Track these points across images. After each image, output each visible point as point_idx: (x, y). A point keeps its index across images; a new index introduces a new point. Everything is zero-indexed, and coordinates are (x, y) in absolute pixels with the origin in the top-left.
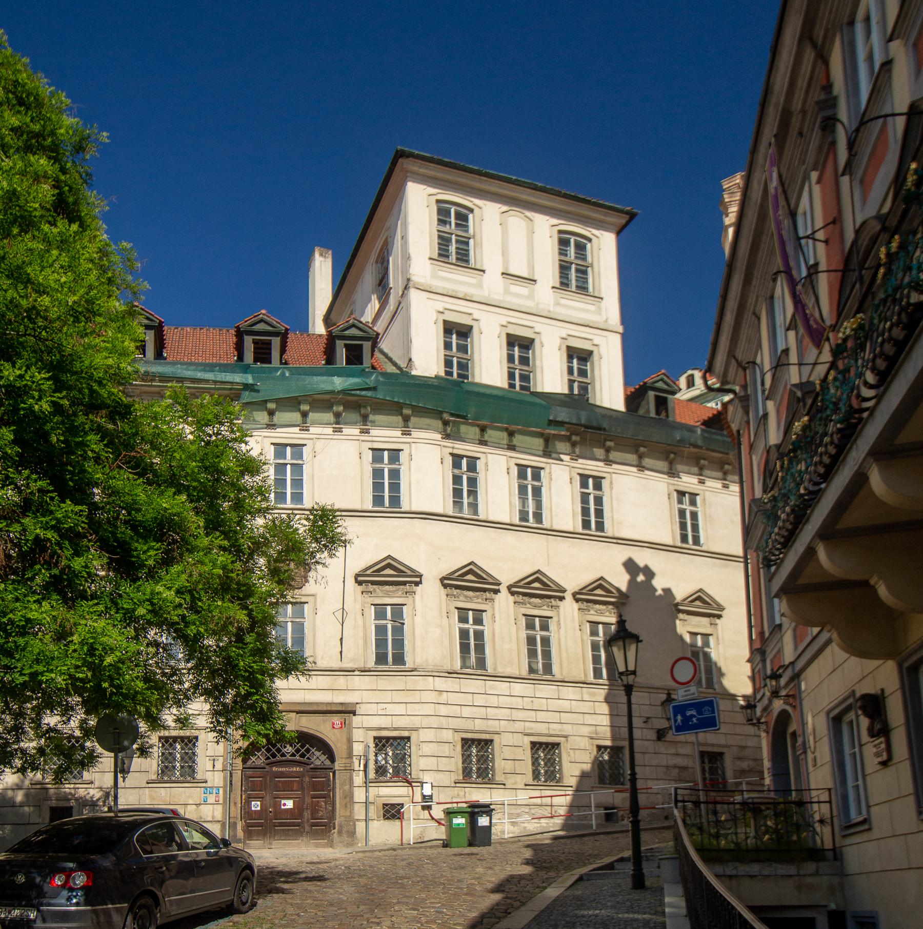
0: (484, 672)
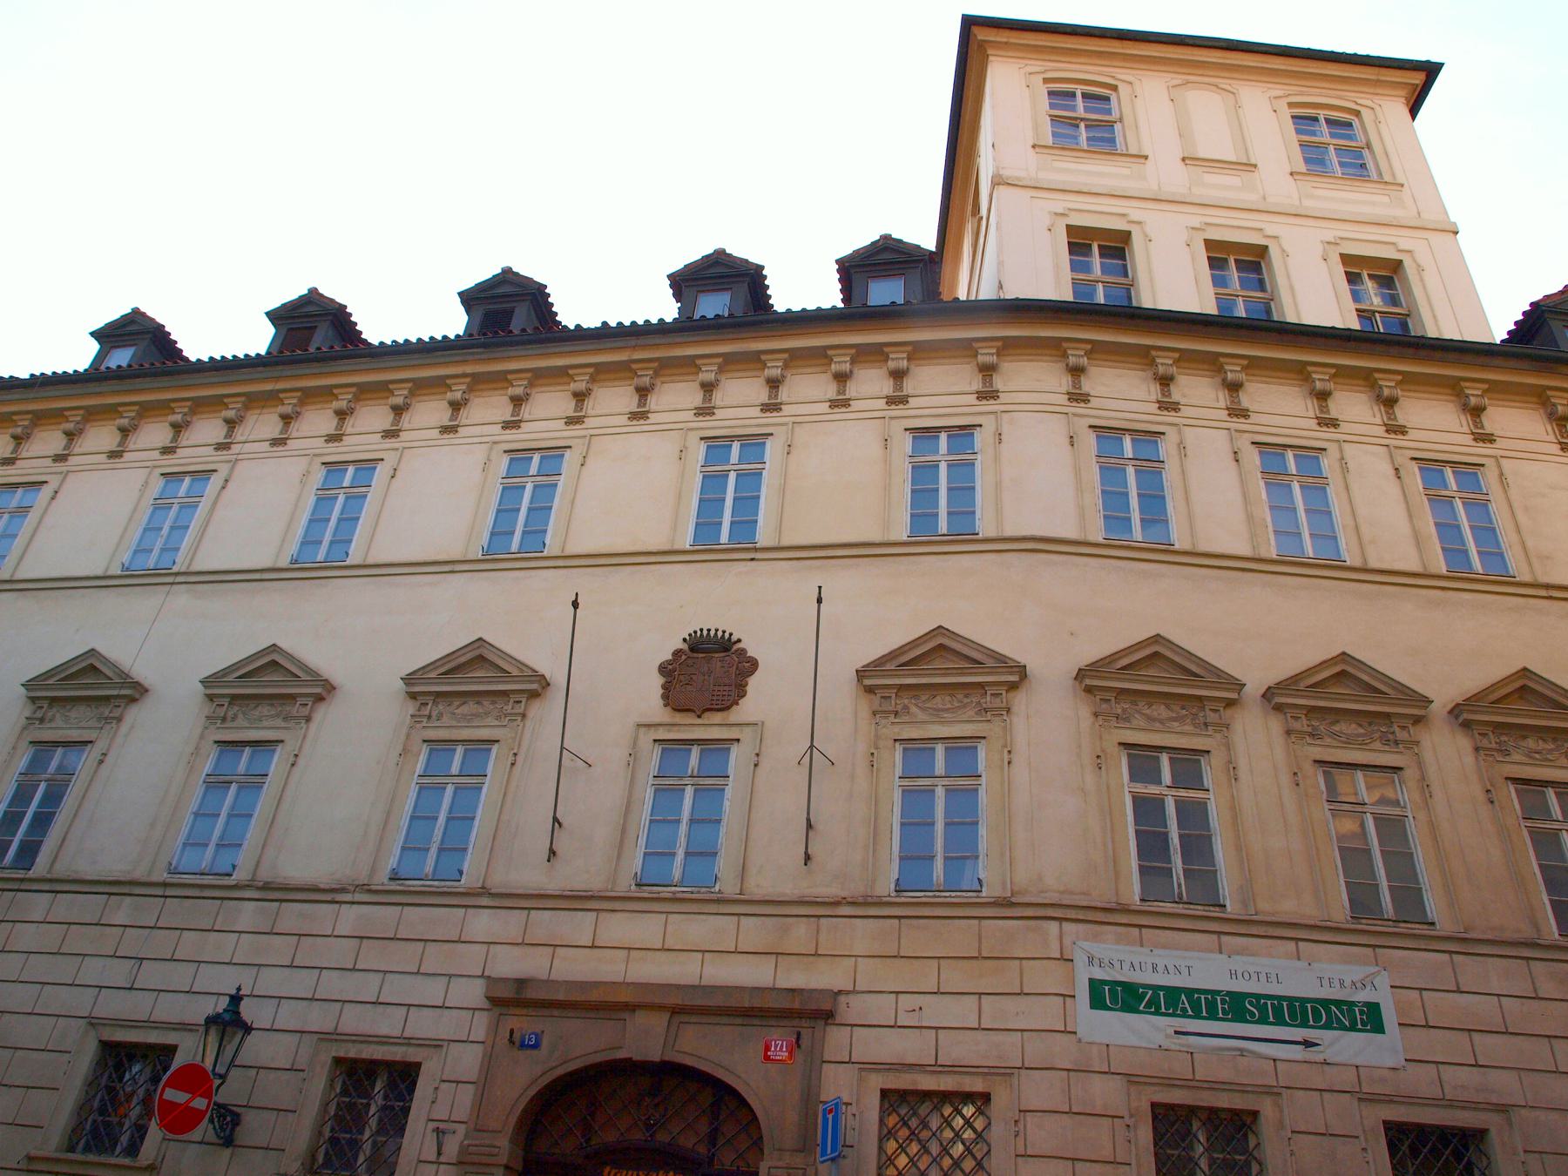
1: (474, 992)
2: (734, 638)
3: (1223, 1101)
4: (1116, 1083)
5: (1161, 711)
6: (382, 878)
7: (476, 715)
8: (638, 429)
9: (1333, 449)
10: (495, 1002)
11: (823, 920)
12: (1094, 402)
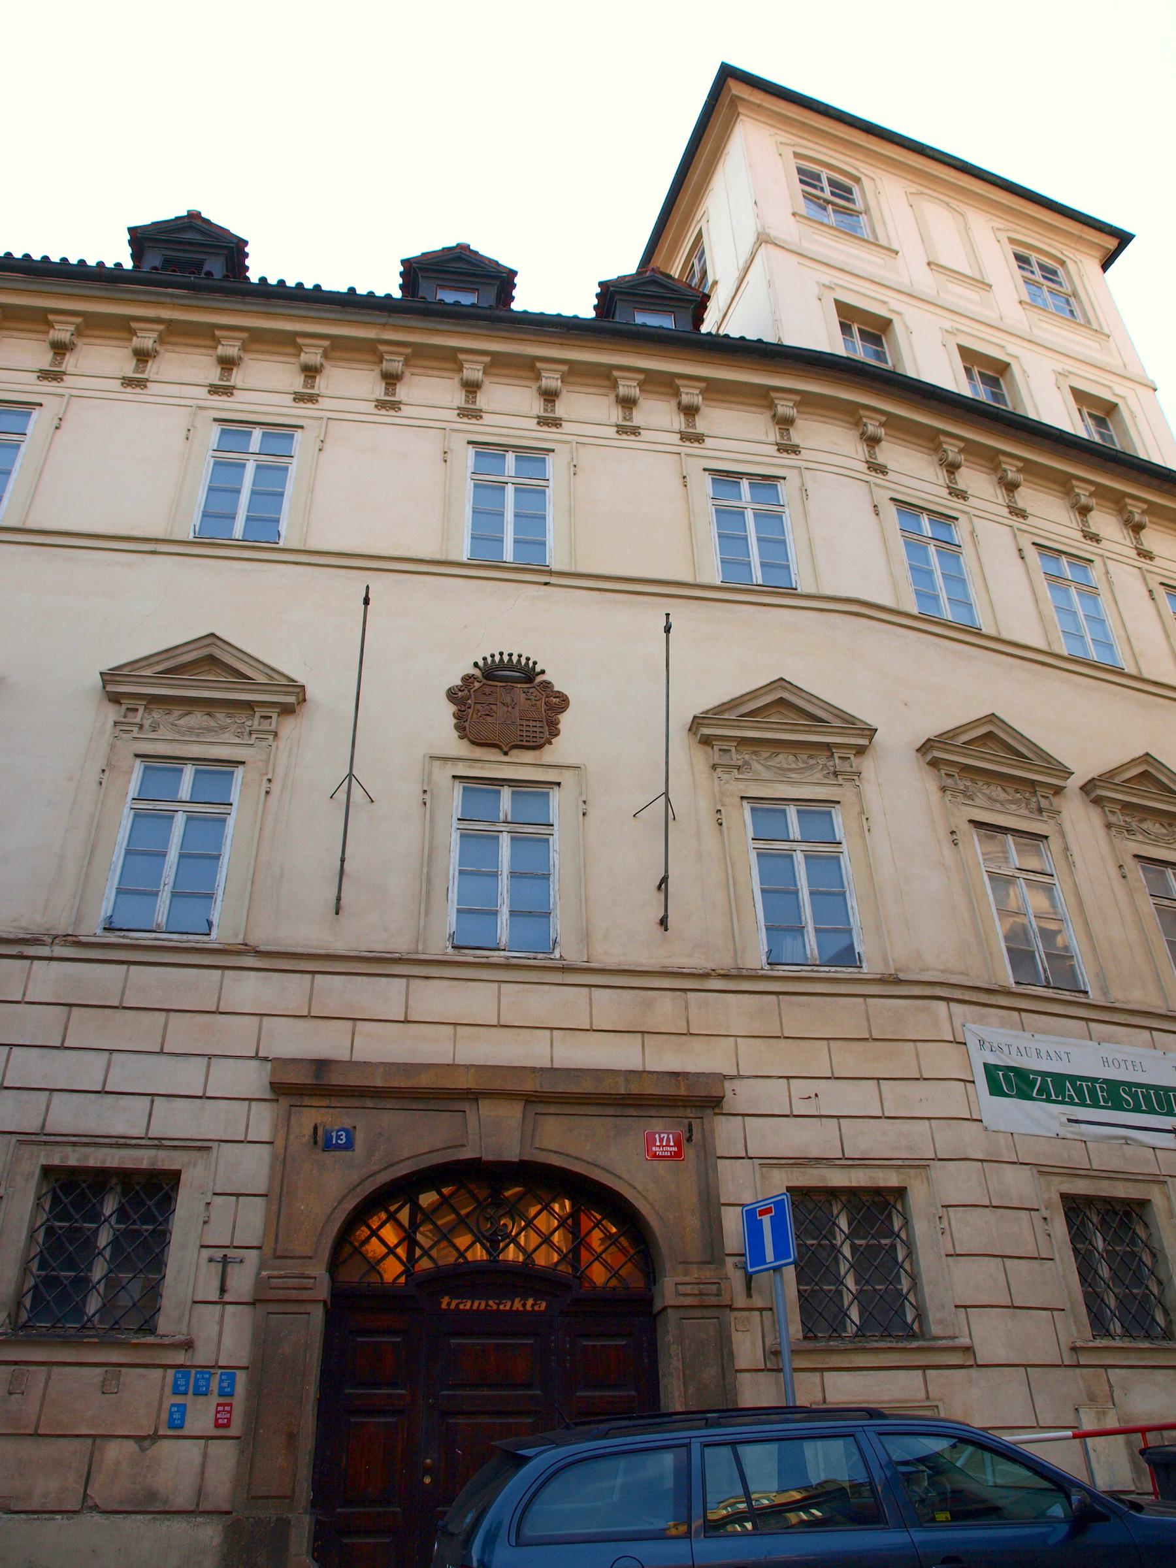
0: (1081, 998)
1: (251, 1079)
2: (538, 668)
3: (1120, 1190)
4: (1025, 1174)
5: (997, 792)
6: (92, 928)
7: (209, 730)
8: (388, 420)
9: (1098, 561)
10: (281, 1090)
11: (690, 994)
12: (891, 476)
